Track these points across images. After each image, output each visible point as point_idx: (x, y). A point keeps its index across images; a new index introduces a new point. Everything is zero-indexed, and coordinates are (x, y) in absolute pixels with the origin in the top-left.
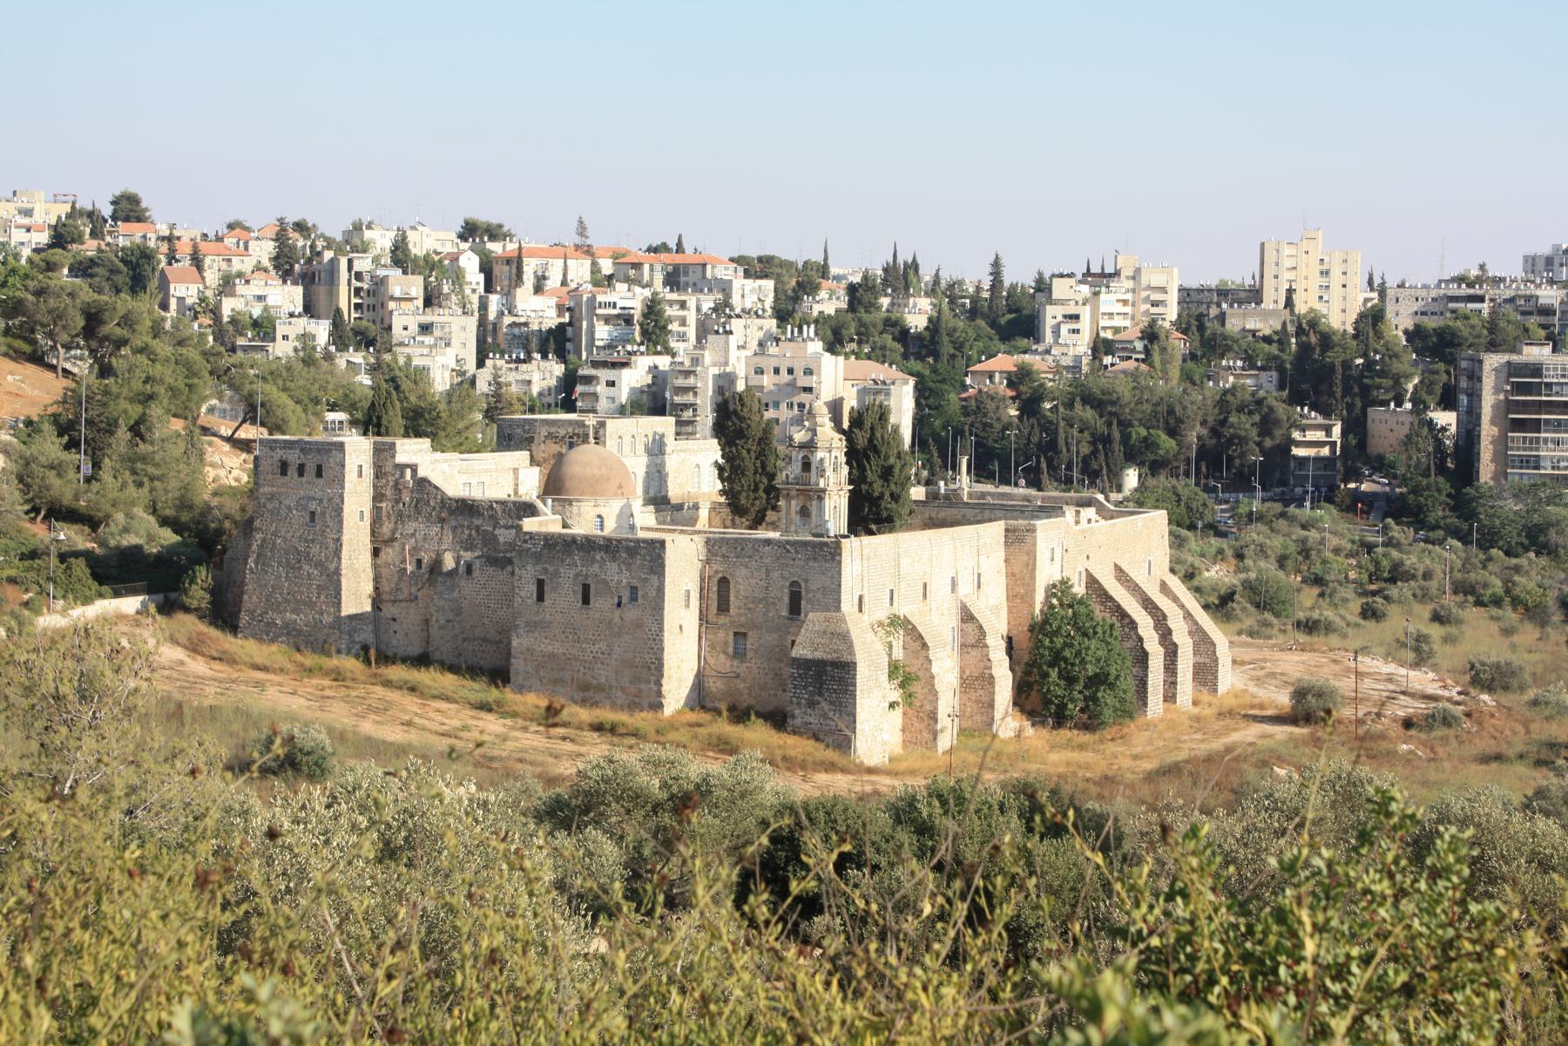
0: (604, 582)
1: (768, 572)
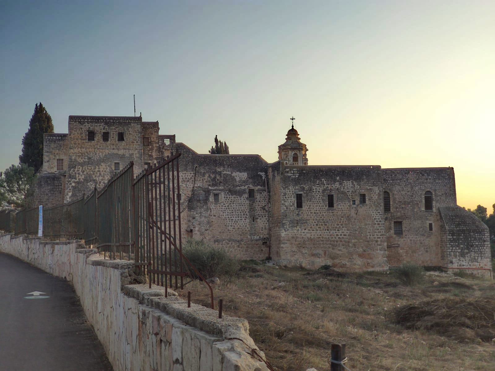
0: (343, 193)
1: (412, 188)
